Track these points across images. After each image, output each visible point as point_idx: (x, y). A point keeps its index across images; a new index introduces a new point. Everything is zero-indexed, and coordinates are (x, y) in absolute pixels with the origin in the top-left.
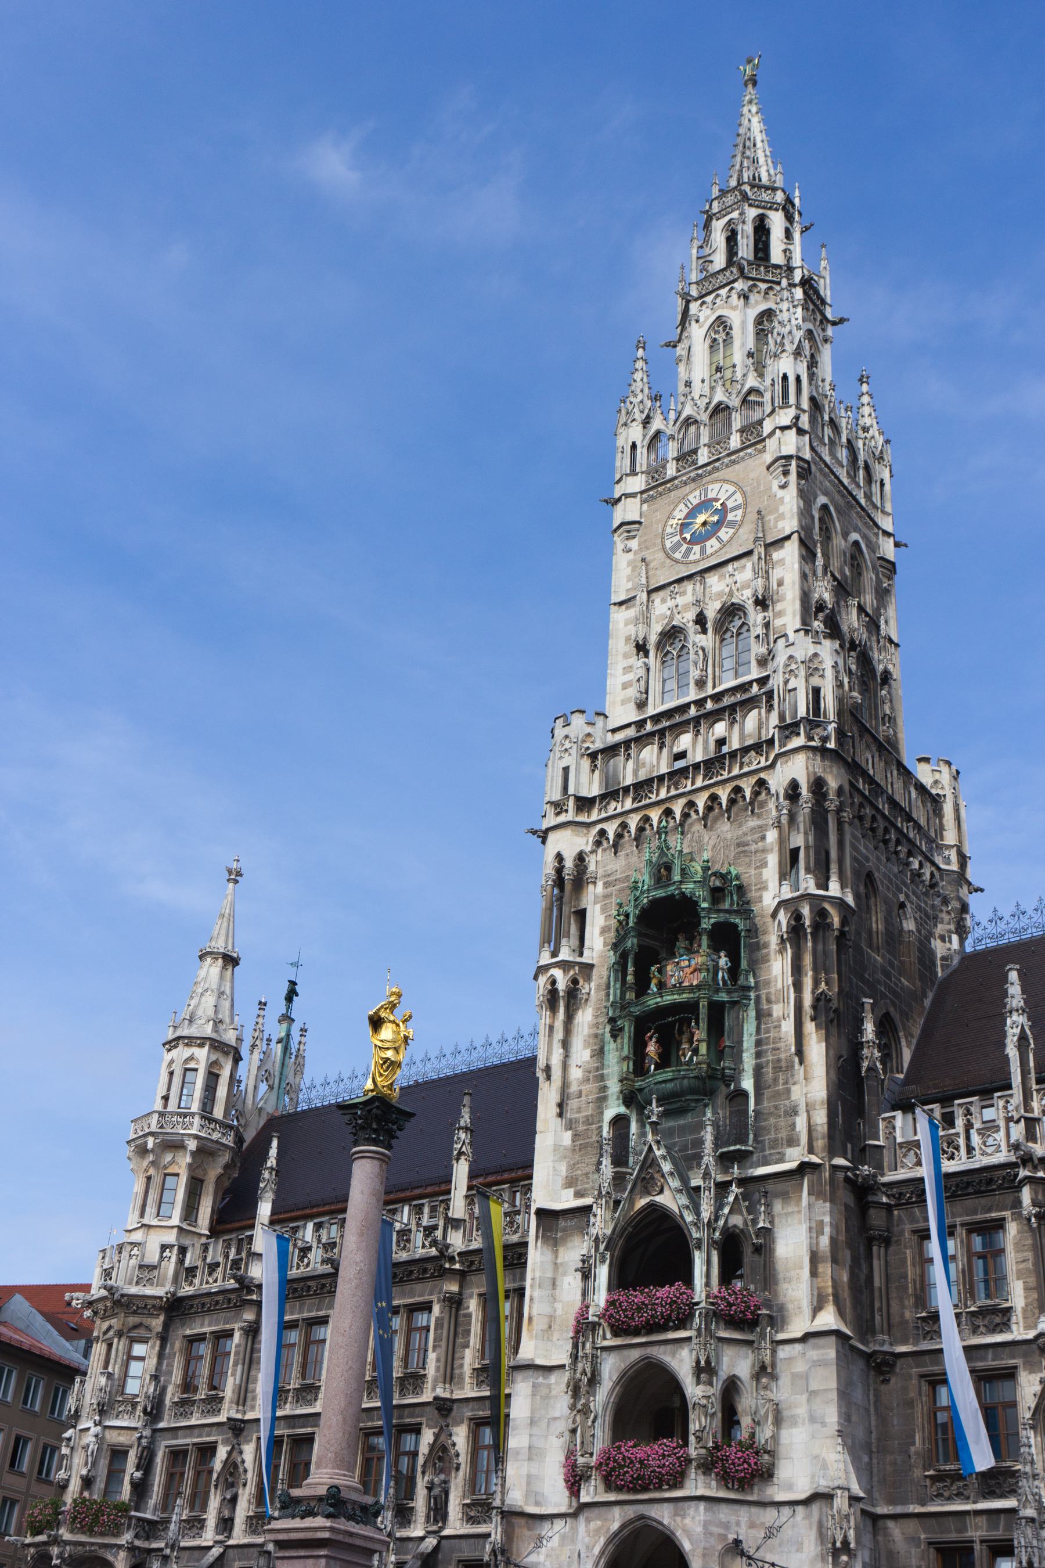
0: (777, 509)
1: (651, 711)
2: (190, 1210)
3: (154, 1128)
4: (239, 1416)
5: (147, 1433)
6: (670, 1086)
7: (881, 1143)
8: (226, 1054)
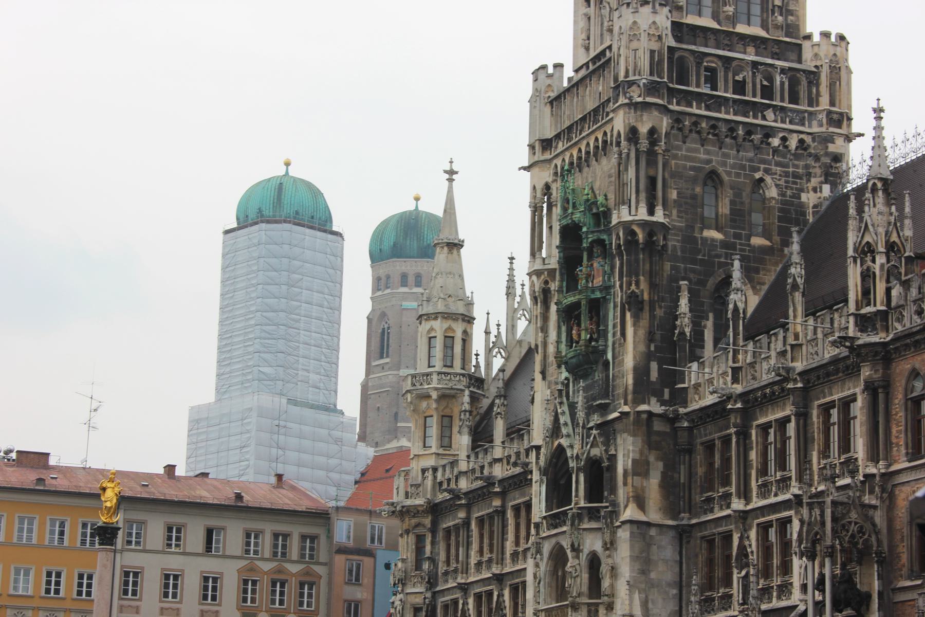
1: (593, 54)
2: (446, 441)
3: (409, 387)
4: (463, 581)
5: (429, 595)
6: (574, 360)
7: (686, 385)
8: (456, 320)
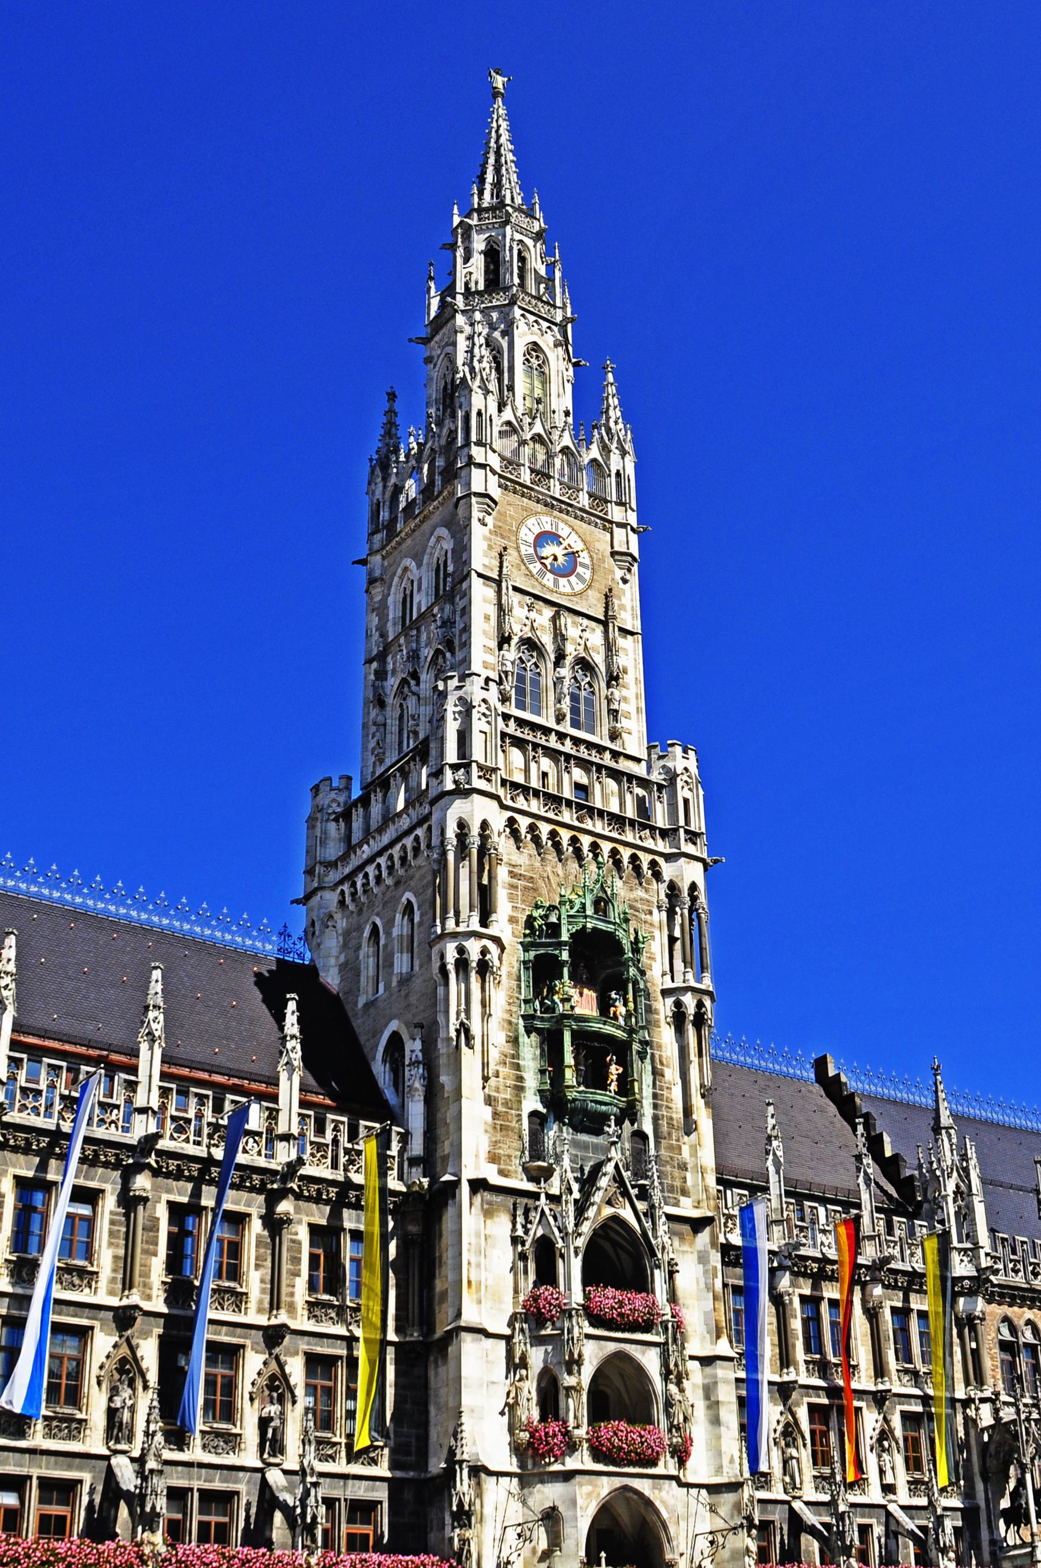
0: (620, 599)
